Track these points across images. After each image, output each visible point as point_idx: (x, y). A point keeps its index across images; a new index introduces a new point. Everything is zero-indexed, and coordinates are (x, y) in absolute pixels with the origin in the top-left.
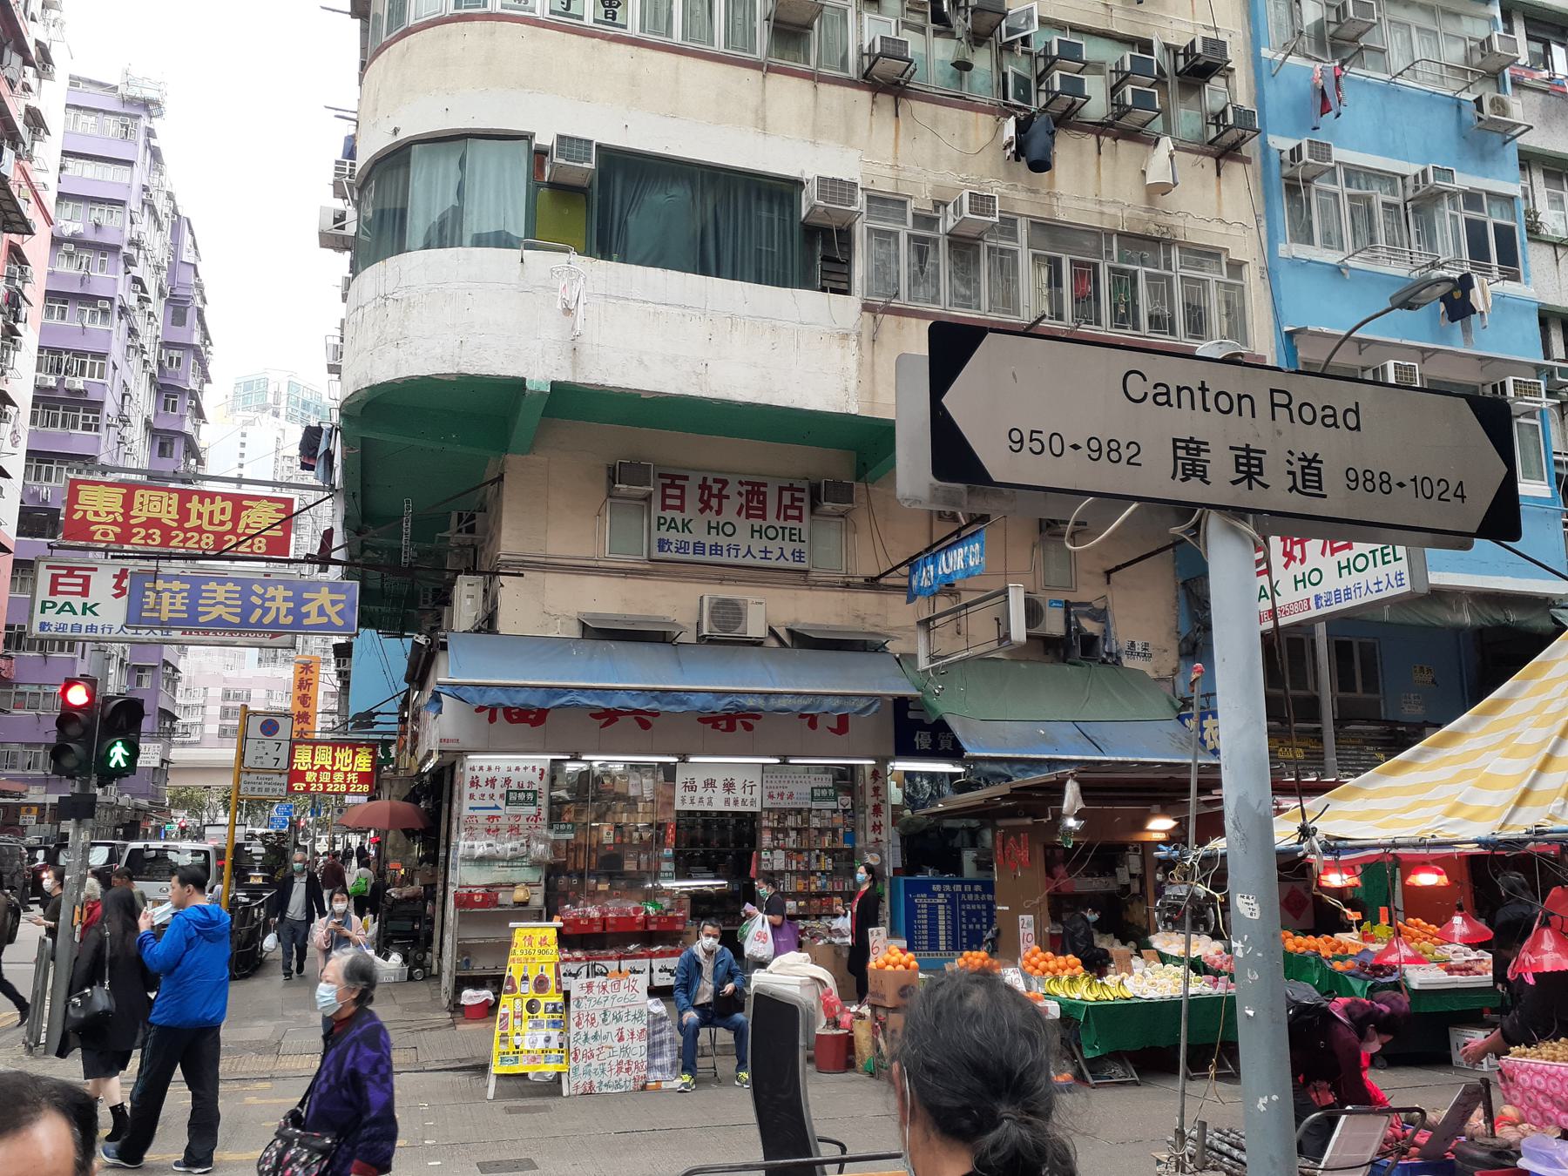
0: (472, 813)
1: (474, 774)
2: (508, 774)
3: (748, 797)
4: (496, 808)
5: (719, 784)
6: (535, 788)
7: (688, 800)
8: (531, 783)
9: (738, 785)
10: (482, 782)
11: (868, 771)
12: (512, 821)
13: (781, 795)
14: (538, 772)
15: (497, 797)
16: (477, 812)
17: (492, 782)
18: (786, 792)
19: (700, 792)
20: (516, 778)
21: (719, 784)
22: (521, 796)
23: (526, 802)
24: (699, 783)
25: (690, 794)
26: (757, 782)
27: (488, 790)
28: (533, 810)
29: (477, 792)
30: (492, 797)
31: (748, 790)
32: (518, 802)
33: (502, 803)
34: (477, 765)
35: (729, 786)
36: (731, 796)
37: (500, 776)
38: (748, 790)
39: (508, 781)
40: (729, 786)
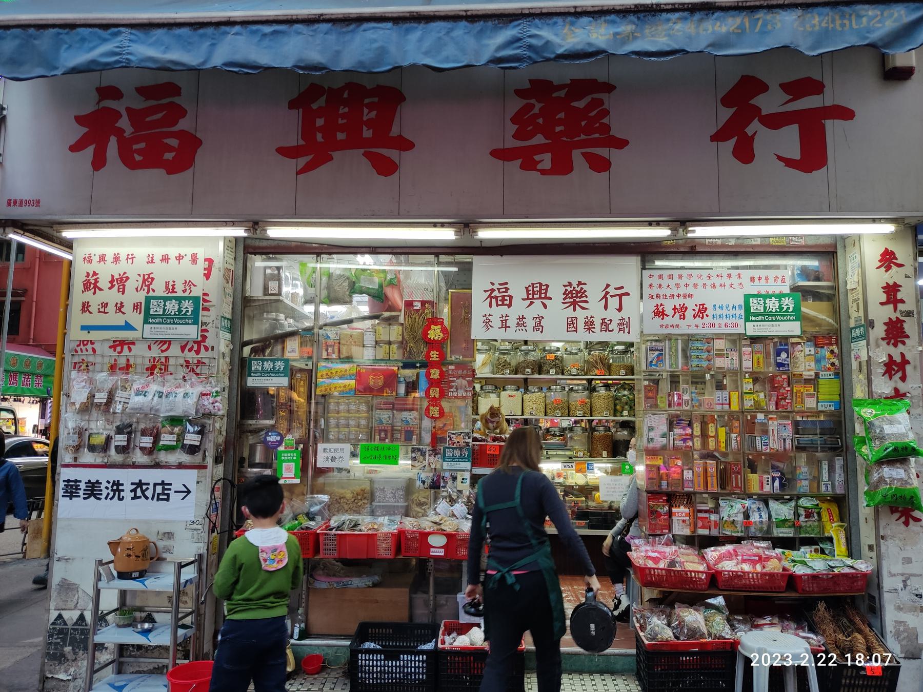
0: (84, 336)
1: (90, 268)
2: (147, 269)
3: (612, 314)
4: (128, 327)
5: (556, 292)
6: (197, 292)
7: (496, 322)
8: (189, 284)
9: (594, 293)
10: (104, 283)
11: (872, 253)
12: (155, 352)
13: (681, 311)
14: (202, 264)
15: (128, 308)
16: (94, 335)
17: (119, 283)
18: (690, 304)
19: (519, 307)
20: (162, 275)
21: (556, 292)
22: (172, 307)
23: (180, 318)
24: (518, 291)
25: (498, 312)
26: (632, 287)
27: (112, 297)
28: (191, 332)
29: (95, 300)
30: (120, 308)
31: (613, 303)
32: (166, 318)
33: (137, 319)
34: (97, 251)
35: (575, 297)
36: (580, 314)
37: (135, 272)
38: (613, 303)
39: (148, 280)
40: (575, 297)
